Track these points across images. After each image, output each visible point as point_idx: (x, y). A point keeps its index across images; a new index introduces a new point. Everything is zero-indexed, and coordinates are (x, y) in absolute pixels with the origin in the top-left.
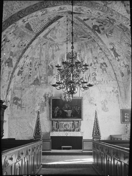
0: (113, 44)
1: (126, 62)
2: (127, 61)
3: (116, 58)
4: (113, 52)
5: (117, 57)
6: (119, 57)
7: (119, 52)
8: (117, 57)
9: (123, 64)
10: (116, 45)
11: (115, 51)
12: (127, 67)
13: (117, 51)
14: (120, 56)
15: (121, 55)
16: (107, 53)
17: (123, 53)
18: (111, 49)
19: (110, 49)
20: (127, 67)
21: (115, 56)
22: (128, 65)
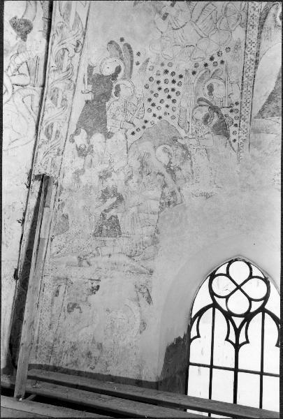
0: (125, 54)
1: (122, 176)
2: (130, 177)
3: (77, 133)
4: (90, 97)
5: (90, 134)
6: (98, 138)
7: (120, 117)
8: (90, 134)
9: (95, 181)
10: (139, 78)
11: (107, 96)
12: (110, 201)
13: (113, 105)
14: (108, 135)
15: (119, 136)
16: (61, 86)
17: (138, 135)
18: (96, 71)
19: (91, 68)
20: (110, 201)
21: (82, 123)
22: (120, 199)
